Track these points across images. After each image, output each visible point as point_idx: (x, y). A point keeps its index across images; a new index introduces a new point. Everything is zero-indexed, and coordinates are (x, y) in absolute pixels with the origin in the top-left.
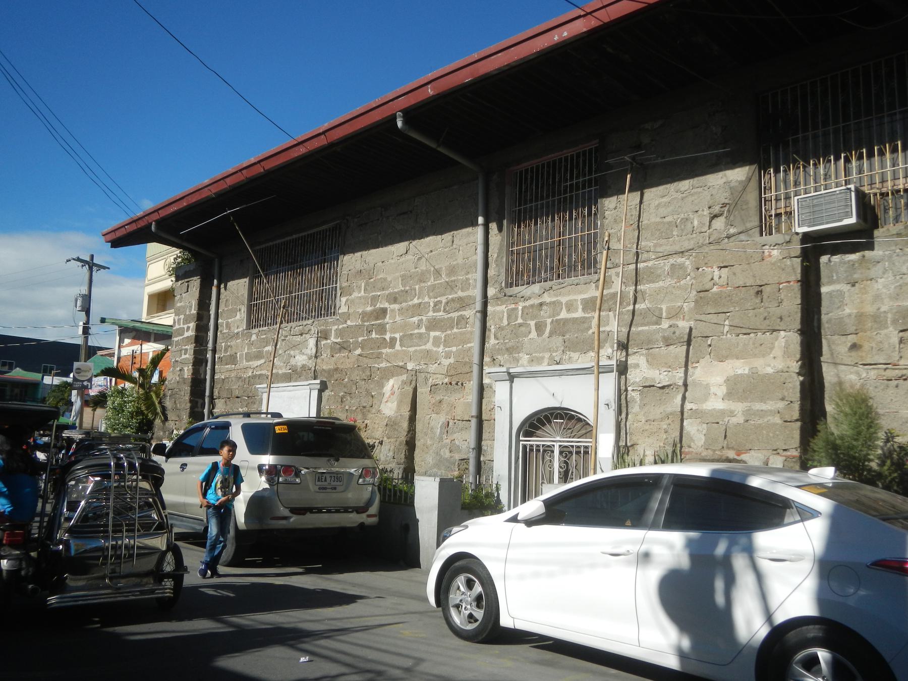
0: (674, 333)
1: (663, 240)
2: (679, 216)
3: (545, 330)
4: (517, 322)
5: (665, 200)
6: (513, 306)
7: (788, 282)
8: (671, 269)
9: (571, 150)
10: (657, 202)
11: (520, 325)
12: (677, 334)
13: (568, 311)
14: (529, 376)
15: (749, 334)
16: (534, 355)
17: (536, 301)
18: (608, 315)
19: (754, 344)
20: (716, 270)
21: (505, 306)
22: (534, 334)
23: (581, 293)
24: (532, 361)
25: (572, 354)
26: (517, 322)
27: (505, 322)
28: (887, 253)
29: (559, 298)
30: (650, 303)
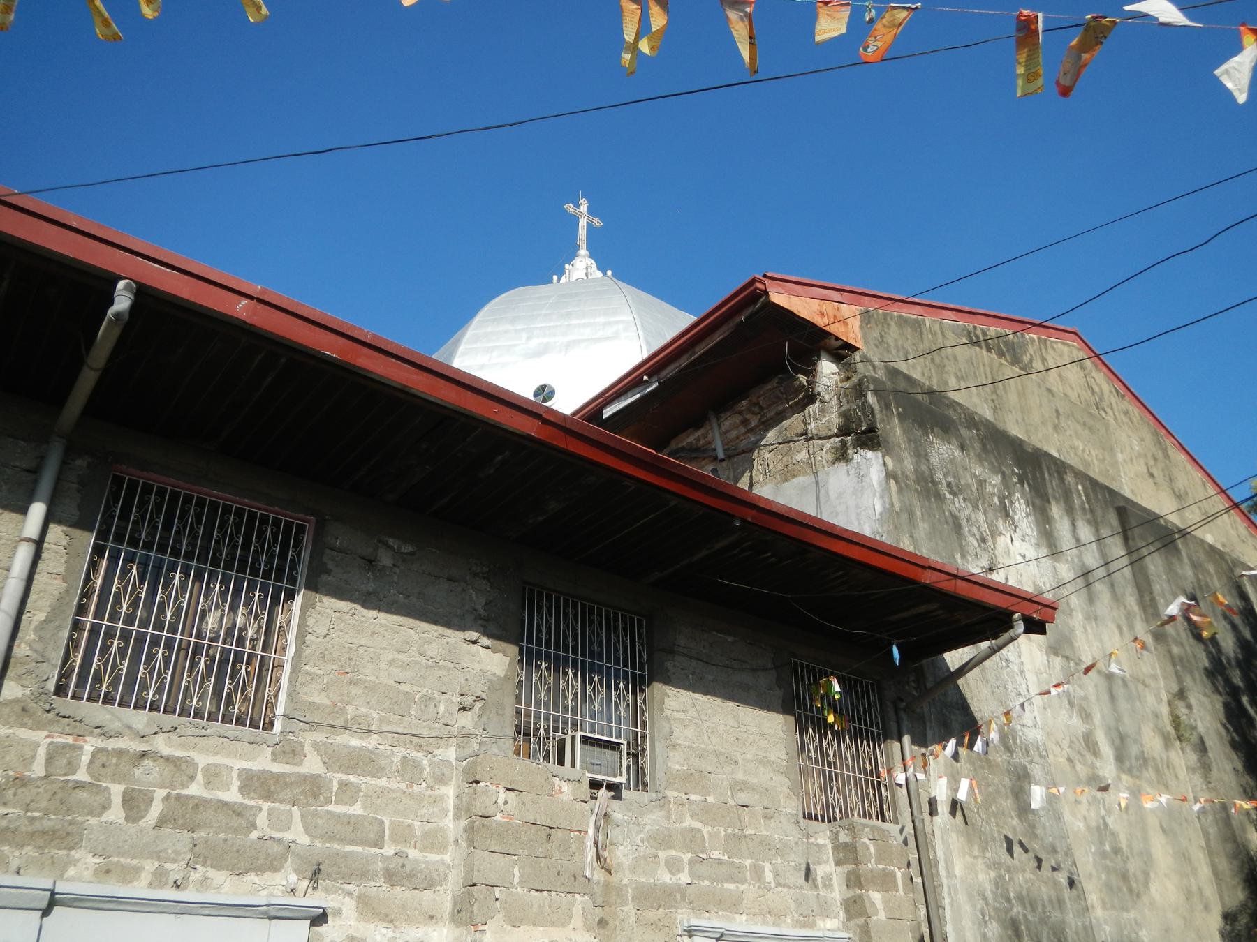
0: (403, 866)
1: (395, 716)
2: (420, 689)
3: (147, 810)
4: (72, 778)
5: (401, 657)
6: (70, 740)
7: (579, 831)
8: (402, 763)
9: (258, 504)
10: (390, 657)
11: (79, 786)
12: (408, 868)
13: (208, 784)
14: (101, 905)
15: (541, 891)
16: (115, 859)
17: (137, 746)
18: (290, 811)
19: (550, 907)
20: (502, 790)
21: (45, 733)
22: (116, 813)
23: (243, 756)
24: (108, 871)
25: (212, 873)
26: (72, 778)
27: (38, 769)
28: (626, 818)
29: (192, 754)
30: (365, 808)
